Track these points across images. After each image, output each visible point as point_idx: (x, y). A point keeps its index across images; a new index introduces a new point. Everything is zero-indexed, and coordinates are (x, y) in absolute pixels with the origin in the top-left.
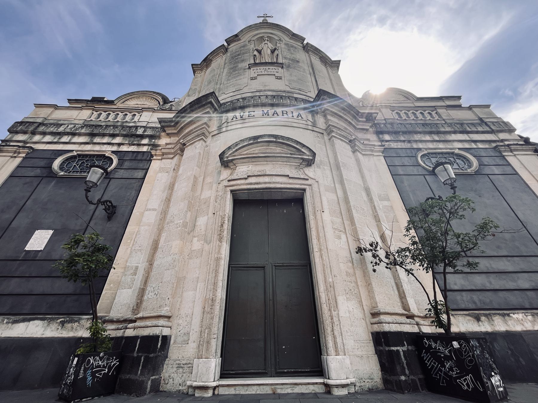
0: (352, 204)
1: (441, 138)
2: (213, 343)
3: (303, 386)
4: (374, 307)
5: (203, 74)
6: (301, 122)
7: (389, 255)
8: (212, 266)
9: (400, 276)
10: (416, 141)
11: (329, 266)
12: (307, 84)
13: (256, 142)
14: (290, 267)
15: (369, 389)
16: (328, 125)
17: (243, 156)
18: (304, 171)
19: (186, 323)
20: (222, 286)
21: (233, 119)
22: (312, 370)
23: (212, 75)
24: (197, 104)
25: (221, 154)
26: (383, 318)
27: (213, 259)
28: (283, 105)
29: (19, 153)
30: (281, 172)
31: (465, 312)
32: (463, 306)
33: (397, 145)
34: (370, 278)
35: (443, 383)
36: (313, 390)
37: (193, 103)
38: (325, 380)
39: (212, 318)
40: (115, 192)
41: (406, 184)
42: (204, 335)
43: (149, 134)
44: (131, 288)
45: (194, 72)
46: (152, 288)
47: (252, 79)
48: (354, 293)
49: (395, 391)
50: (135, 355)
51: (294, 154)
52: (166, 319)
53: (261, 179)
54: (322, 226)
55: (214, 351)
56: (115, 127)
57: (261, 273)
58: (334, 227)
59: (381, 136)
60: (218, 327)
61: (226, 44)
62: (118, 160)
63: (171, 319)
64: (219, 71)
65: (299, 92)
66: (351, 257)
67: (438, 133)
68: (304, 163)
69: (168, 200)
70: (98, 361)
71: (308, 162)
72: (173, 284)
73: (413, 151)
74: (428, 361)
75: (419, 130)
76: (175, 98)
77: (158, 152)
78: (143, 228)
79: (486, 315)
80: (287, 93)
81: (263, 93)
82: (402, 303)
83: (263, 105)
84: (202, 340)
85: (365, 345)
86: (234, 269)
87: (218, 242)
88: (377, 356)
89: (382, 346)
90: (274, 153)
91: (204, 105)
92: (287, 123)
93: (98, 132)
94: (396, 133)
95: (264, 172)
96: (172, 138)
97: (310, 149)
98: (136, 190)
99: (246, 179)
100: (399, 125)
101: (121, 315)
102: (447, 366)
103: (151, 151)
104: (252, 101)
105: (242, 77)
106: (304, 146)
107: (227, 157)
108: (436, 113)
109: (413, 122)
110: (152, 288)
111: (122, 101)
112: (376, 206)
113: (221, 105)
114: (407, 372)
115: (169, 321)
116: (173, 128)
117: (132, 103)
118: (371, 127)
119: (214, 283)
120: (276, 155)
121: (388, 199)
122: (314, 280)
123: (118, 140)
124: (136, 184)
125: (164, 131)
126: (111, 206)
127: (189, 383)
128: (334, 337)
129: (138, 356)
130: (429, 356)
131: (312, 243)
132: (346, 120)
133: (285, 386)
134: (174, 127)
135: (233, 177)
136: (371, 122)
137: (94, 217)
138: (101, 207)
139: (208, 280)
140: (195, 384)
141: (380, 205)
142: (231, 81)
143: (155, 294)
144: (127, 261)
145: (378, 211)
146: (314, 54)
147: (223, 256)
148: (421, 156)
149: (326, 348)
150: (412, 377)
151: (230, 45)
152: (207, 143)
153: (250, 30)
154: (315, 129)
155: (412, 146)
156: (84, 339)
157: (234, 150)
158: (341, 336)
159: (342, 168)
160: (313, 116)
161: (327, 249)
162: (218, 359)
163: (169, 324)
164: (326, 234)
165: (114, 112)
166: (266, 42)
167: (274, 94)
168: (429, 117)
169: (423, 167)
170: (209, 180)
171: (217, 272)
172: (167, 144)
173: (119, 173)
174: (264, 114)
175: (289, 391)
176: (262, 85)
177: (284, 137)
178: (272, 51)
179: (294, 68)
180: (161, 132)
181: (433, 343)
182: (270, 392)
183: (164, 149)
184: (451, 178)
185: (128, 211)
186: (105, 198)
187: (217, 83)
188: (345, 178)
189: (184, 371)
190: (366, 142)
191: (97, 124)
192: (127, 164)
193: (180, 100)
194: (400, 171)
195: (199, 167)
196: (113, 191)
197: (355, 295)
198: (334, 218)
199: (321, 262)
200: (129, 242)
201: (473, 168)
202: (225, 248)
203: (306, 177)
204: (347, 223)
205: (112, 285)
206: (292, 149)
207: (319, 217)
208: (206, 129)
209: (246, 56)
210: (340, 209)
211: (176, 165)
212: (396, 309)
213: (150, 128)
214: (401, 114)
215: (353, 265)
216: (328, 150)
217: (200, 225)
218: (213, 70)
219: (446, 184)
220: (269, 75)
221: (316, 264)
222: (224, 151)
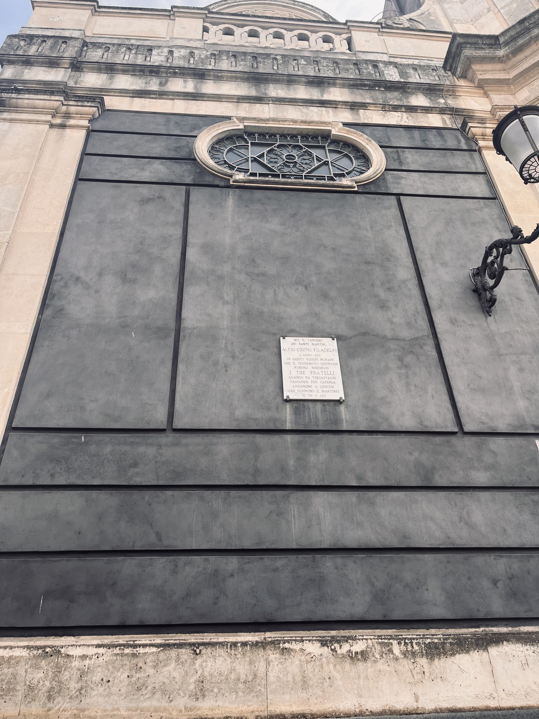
29: (67, 115)
43: (422, 81)
116: (499, 66)
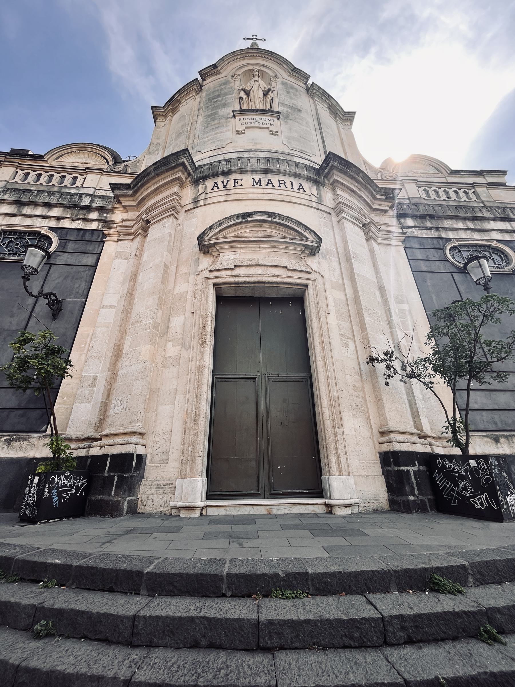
0: (363, 305)
3: (302, 506)
4: (383, 426)
5: (168, 121)
6: (303, 196)
7: (406, 366)
9: (414, 392)
10: (446, 229)
11: (333, 378)
12: (312, 144)
13: (245, 221)
15: (374, 510)
16: (337, 202)
17: (229, 240)
18: (306, 262)
19: (163, 441)
21: (213, 189)
22: (311, 491)
23: (180, 124)
24: (165, 165)
25: (200, 235)
26: (393, 436)
27: (194, 367)
28: (280, 173)
31: (483, 434)
32: (482, 427)
33: (421, 234)
34: (380, 392)
35: (454, 503)
36: (313, 511)
37: (158, 164)
38: (327, 500)
39: (196, 435)
40: (58, 283)
41: (429, 282)
42: (188, 454)
43: (99, 205)
44: (90, 402)
45: (155, 118)
46: (118, 401)
47: (238, 134)
49: (401, 511)
50: (106, 474)
51: (295, 239)
52: (139, 437)
55: (200, 470)
56: (51, 193)
57: (251, 385)
59: (402, 220)
61: (200, 78)
63: (145, 437)
65: (301, 154)
66: (360, 369)
67: (474, 219)
68: (306, 252)
69: (130, 295)
70: (64, 480)
71: (312, 250)
74: (440, 482)
75: (450, 214)
76: (130, 156)
77: (113, 232)
78: (99, 329)
79: (506, 437)
80: (285, 156)
82: (415, 422)
83: (254, 171)
85: (372, 465)
86: (219, 380)
90: (269, 237)
91: (174, 168)
92: (284, 197)
93: (27, 200)
94: (422, 217)
96: (130, 213)
98: (86, 280)
99: (232, 269)
100: (427, 207)
101: (81, 433)
102: (461, 486)
103: (104, 229)
104: (239, 165)
105: (224, 129)
106: (307, 228)
107: (209, 240)
108: (474, 192)
109: (444, 203)
110: (118, 401)
111: (55, 157)
113: (197, 168)
114: (417, 492)
116: (131, 199)
117: (70, 160)
118: (391, 207)
120: (271, 239)
122: (315, 393)
123: (56, 212)
125: (119, 202)
127: (172, 504)
128: (338, 456)
129: (109, 475)
130: (441, 476)
131: (314, 352)
132: (360, 197)
133: (282, 506)
135: (216, 267)
138: (43, 302)
139: (189, 392)
140: (179, 504)
142: (209, 134)
144: (82, 370)
146: (322, 101)
147: (207, 364)
148: (450, 249)
149: (329, 467)
151: (205, 80)
153: (233, 58)
155: (441, 235)
157: (217, 230)
159: (353, 260)
160: (318, 189)
164: (332, 341)
166: (256, 78)
167: (268, 155)
168: (464, 198)
169: (452, 263)
170: (183, 269)
171: (199, 382)
172: (123, 220)
173: (62, 258)
174: (255, 184)
175: (286, 511)
176: (252, 143)
182: (265, 512)
183: (120, 226)
184: (485, 277)
185: (78, 308)
186: (46, 290)
187: (189, 136)
188: (357, 273)
189: (165, 492)
190: (383, 228)
191: (25, 188)
192: (71, 246)
195: (169, 253)
196: (57, 282)
199: (325, 373)
201: (511, 266)
202: (208, 355)
203: (309, 270)
204: (356, 328)
205: (65, 398)
206: (292, 232)
207: (323, 320)
210: (349, 311)
211: (138, 249)
213: (99, 197)
214: (430, 192)
215: (361, 377)
216: (336, 236)
217: (175, 327)
218: (183, 116)
219: (479, 284)
220: (260, 128)
222: (204, 232)
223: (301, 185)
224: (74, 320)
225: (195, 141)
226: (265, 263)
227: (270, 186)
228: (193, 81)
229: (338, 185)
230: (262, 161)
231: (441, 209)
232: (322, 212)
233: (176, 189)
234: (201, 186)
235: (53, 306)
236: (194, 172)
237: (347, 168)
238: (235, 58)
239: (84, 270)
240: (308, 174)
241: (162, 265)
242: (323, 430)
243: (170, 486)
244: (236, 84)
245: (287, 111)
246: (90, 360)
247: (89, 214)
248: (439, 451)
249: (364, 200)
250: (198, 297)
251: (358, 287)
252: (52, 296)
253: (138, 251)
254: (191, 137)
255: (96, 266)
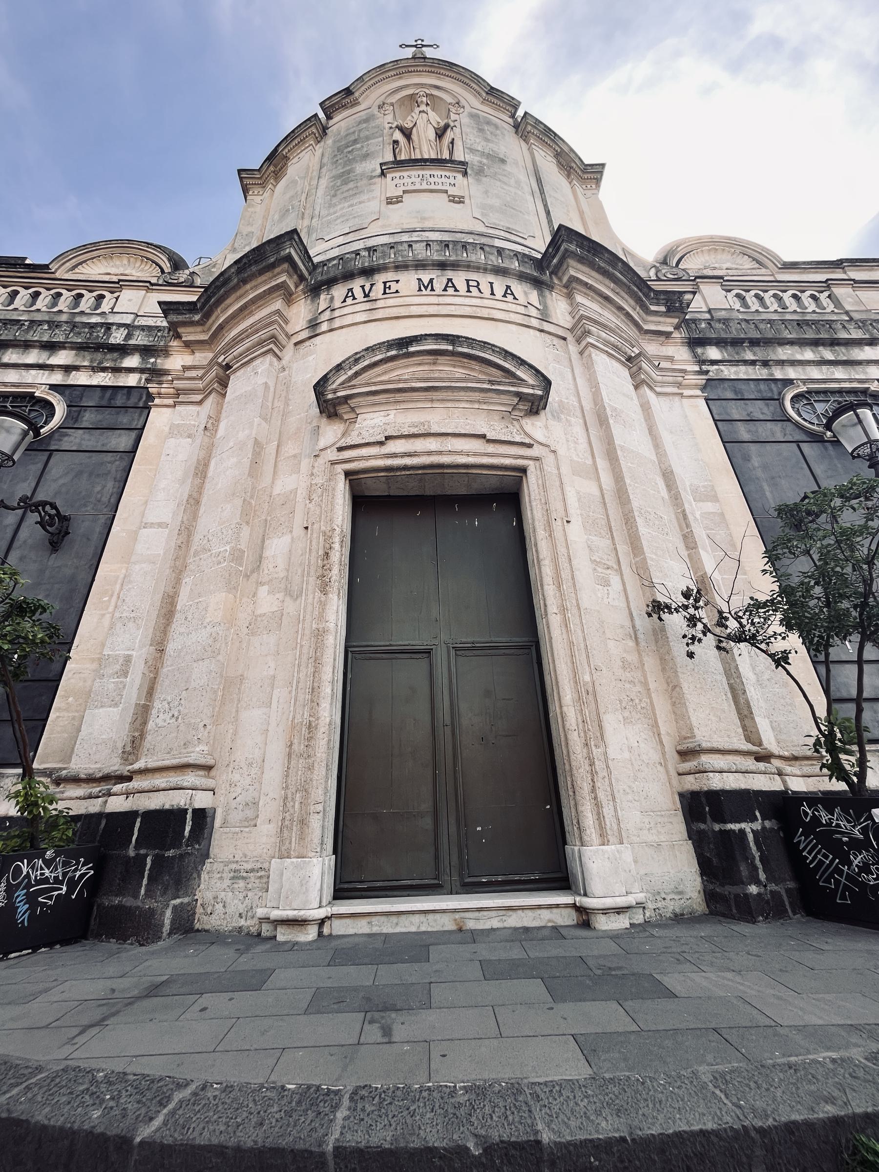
0: (635, 504)
1: (838, 355)
2: (315, 822)
3: (525, 911)
4: (685, 738)
7: (727, 619)
8: (305, 650)
9: (741, 669)
10: (781, 363)
11: (582, 646)
12: (526, 217)
13: (404, 354)
14: (489, 651)
15: (676, 915)
16: (577, 317)
17: (373, 388)
18: (522, 427)
19: (248, 780)
20: (332, 696)
21: (344, 301)
22: (545, 876)
23: (288, 196)
24: (256, 262)
25: (318, 383)
26: (706, 760)
27: (307, 632)
28: (469, 267)
30: (468, 427)
34: (676, 672)
35: (843, 897)
36: (549, 921)
37: (245, 260)
38: (578, 899)
39: (310, 768)
40: (64, 484)
41: (756, 462)
42: (293, 806)
43: (141, 343)
44: (116, 705)
45: (245, 191)
46: (165, 703)
47: (391, 203)
48: (639, 707)
50: (132, 853)
51: (499, 383)
52: (201, 773)
53: (419, 445)
54: (566, 555)
55: (317, 841)
56: (53, 325)
57: (422, 664)
58: (593, 558)
59: (699, 350)
60: (326, 788)
61: (322, 115)
62: (68, 406)
63: (213, 773)
64: (306, 183)
65: (508, 236)
66: (634, 627)
67: (834, 343)
68: (521, 407)
69: (194, 502)
71: (533, 403)
72: (215, 692)
73: (773, 385)
74: (810, 853)
75: (789, 336)
76: (200, 258)
77: (165, 389)
78: (137, 567)
80: (476, 237)
81: (418, 236)
82: (744, 727)
83: (420, 265)
84: (288, 818)
85: (666, 820)
86: (358, 656)
87: (318, 594)
88: (693, 844)
89: (705, 822)
90: (450, 380)
91: (273, 266)
92: (478, 309)
94: (736, 343)
95: (426, 427)
96: (198, 355)
97: (538, 371)
99: (381, 443)
100: (744, 325)
101: (98, 766)
102: (856, 862)
103: (149, 386)
104: (393, 256)
105: (364, 197)
106: (522, 362)
107: (335, 391)
108: (829, 296)
109: (775, 317)
110: (165, 703)
111: (69, 265)
112: (687, 511)
113: (315, 266)
114: (762, 876)
115: (208, 777)
116: (199, 329)
117: (95, 270)
118: (677, 327)
119: (313, 689)
120: (453, 384)
121: (715, 498)
122: (547, 678)
123: (63, 357)
124: (115, 465)
125: (178, 336)
126: (56, 515)
127: (261, 912)
128: (598, 805)
129: (137, 855)
130: (811, 841)
131: (543, 595)
132: (620, 308)
133: (485, 913)
134: (202, 325)
135: (350, 441)
136: (676, 314)
137: (16, 544)
138: (33, 517)
139: (298, 682)
140: (275, 914)
141: (696, 510)
142: (339, 207)
143: (173, 716)
144: (103, 645)
145: (693, 524)
146: (543, 145)
147: (331, 626)
148: (792, 398)
149: (579, 828)
150: (772, 887)
151: (331, 118)
152: (284, 362)
154: (546, 327)
155: (772, 375)
156: (10, 818)
157: (350, 373)
158: (611, 803)
159: (611, 421)
160: (541, 295)
161: (579, 609)
162: (327, 859)
163: (210, 783)
164: (576, 573)
165: (48, 289)
166: (423, 107)
167: (446, 237)
168: (811, 306)
169: (797, 425)
170: (290, 449)
171: (317, 662)
172: (185, 368)
173: (72, 438)
175: (495, 923)
176: (417, 217)
177: (474, 340)
178: (439, 132)
179: (494, 176)
180: (169, 339)
181: (823, 814)
183: (179, 379)
186: (40, 496)
187: (303, 214)
188: (619, 446)
189: (250, 886)
190: (664, 365)
191: (8, 317)
192: (88, 418)
193: (214, 260)
194: (743, 432)
195: (265, 419)
196: (61, 482)
197: (642, 711)
198: (594, 538)
199: (565, 636)
200: (105, 601)
202: (335, 608)
203: (527, 441)
204: (623, 549)
205: (71, 699)
206: (493, 371)
207: (558, 534)
208: (280, 325)
209: (374, 144)
210: (608, 516)
211: (210, 417)
212: (735, 740)
213: (143, 328)
214: (747, 299)
216: (578, 379)
217: (273, 556)
218: (292, 182)
219: (859, 456)
220: (431, 191)
221: (553, 641)
222: (325, 376)
223: (508, 287)
224: (90, 551)
225: (313, 221)
226: (443, 431)
227: (451, 291)
228: (309, 119)
229: (578, 287)
230: (435, 247)
231: (771, 327)
232: (551, 337)
233: (278, 304)
234: (322, 297)
235: (51, 525)
236: (310, 274)
237: (594, 255)
238: (384, 76)
239: (113, 459)
240: (522, 269)
241: (250, 444)
242: (565, 752)
243: (259, 874)
244: (387, 120)
245: (481, 162)
246: (119, 625)
247: (122, 359)
248: (798, 785)
249: (628, 315)
250: (315, 497)
251: (624, 470)
252: (48, 508)
253: (211, 421)
254: (306, 216)
255: (134, 451)
